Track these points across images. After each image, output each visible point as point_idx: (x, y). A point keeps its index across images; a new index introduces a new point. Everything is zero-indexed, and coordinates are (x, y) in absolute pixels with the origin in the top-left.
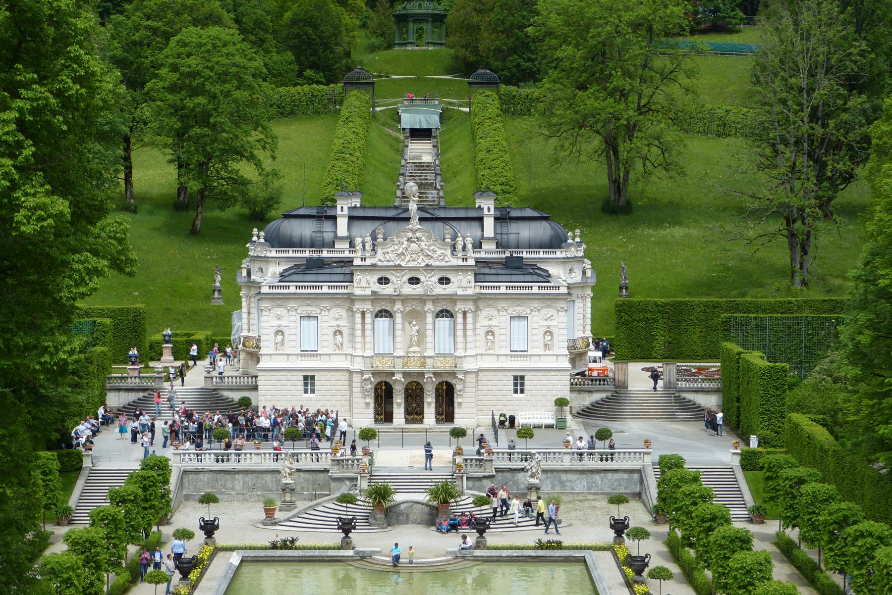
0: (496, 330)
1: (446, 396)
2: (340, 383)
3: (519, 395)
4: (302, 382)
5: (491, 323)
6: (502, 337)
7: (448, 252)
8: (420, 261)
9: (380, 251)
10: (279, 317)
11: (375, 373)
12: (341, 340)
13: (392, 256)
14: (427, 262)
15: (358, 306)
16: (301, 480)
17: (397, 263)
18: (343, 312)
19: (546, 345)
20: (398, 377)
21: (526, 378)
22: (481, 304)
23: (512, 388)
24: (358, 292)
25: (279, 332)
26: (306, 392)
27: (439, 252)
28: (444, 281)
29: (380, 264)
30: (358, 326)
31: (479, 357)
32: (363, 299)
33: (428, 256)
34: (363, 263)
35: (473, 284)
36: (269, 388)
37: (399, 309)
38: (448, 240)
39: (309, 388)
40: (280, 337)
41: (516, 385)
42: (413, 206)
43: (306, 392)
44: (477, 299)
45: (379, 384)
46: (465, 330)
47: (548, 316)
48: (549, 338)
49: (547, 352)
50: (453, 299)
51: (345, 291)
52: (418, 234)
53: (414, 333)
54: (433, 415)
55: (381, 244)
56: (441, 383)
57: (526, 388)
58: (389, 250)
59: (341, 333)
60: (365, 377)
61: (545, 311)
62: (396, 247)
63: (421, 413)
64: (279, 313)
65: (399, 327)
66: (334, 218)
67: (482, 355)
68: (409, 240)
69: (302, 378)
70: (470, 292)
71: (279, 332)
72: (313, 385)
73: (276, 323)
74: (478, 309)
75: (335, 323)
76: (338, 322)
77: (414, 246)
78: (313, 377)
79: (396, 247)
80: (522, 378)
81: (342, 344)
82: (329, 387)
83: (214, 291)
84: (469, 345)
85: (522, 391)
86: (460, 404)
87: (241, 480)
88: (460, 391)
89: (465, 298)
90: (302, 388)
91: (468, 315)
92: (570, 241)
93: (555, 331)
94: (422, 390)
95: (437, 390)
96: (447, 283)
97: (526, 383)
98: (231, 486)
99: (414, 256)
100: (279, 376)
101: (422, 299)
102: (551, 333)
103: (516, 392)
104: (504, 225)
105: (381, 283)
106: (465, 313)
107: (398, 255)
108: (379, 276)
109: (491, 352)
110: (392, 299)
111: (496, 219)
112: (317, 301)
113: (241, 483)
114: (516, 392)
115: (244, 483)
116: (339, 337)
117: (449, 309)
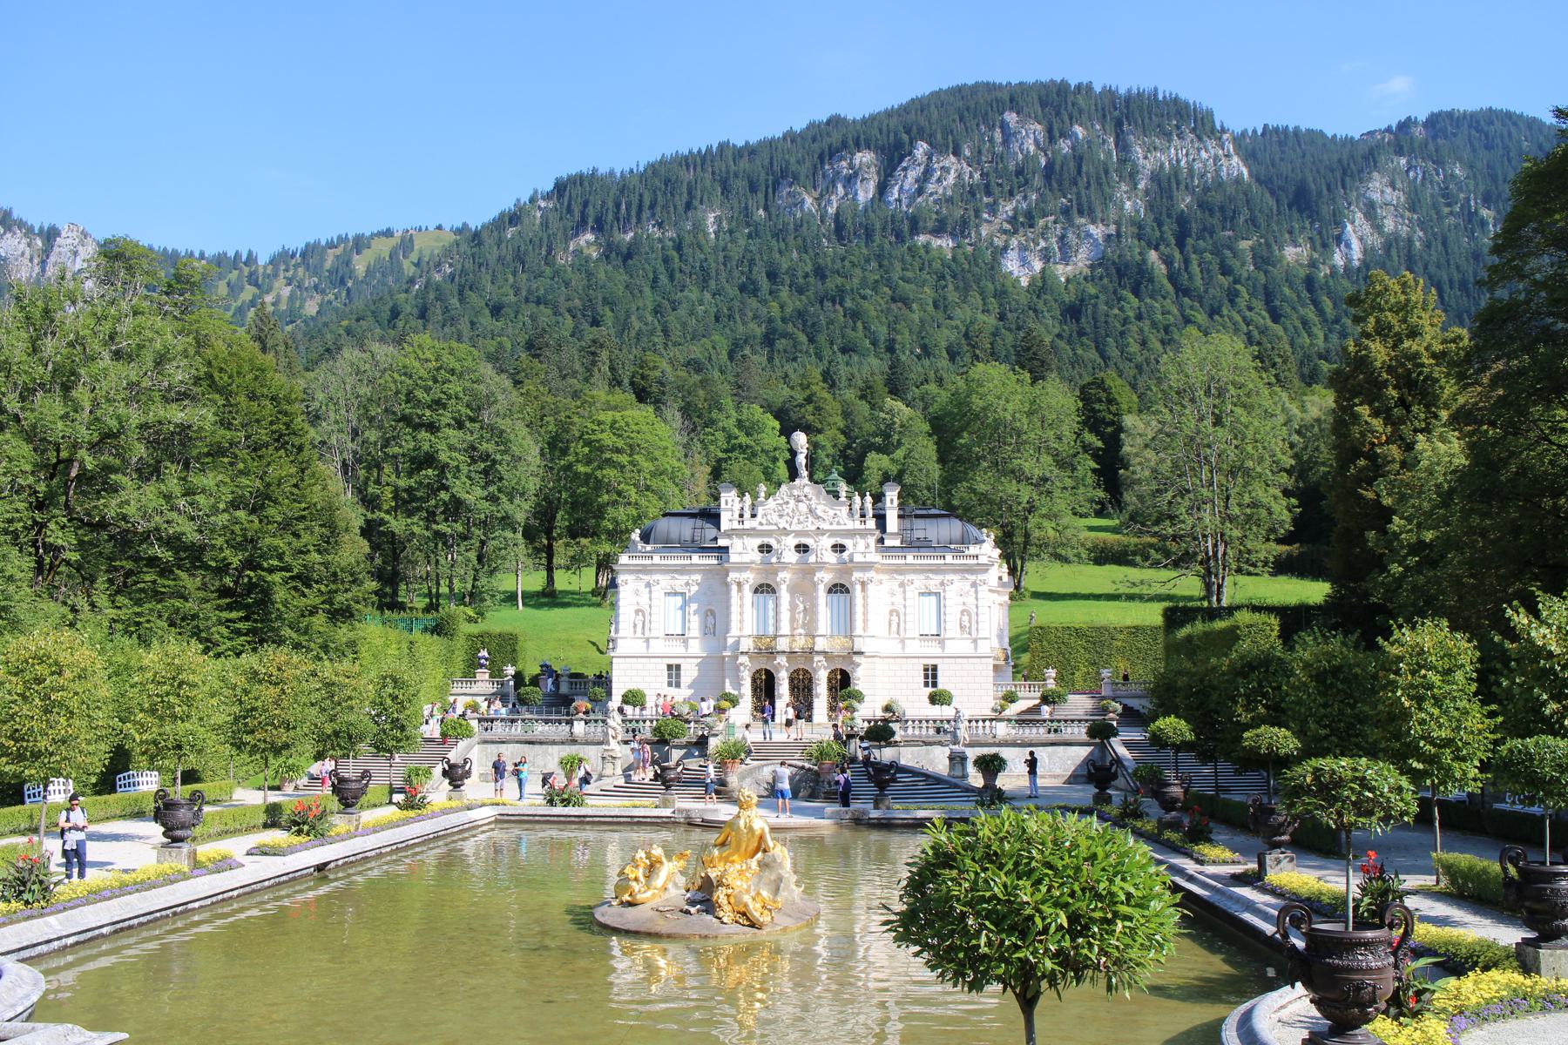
1: (842, 683)
5: (894, 599)
7: (845, 509)
10: (637, 592)
13: (775, 518)
20: (782, 660)
26: (670, 684)
27: (831, 513)
33: (818, 518)
41: (926, 676)
43: (670, 684)
63: (810, 707)
72: (678, 676)
77: (803, 507)
78: (678, 667)
80: (935, 668)
90: (666, 679)
91: (870, 587)
94: (810, 680)
97: (940, 673)
102: (969, 615)
104: (907, 522)
106: (863, 584)
108: (759, 541)
111: (900, 517)
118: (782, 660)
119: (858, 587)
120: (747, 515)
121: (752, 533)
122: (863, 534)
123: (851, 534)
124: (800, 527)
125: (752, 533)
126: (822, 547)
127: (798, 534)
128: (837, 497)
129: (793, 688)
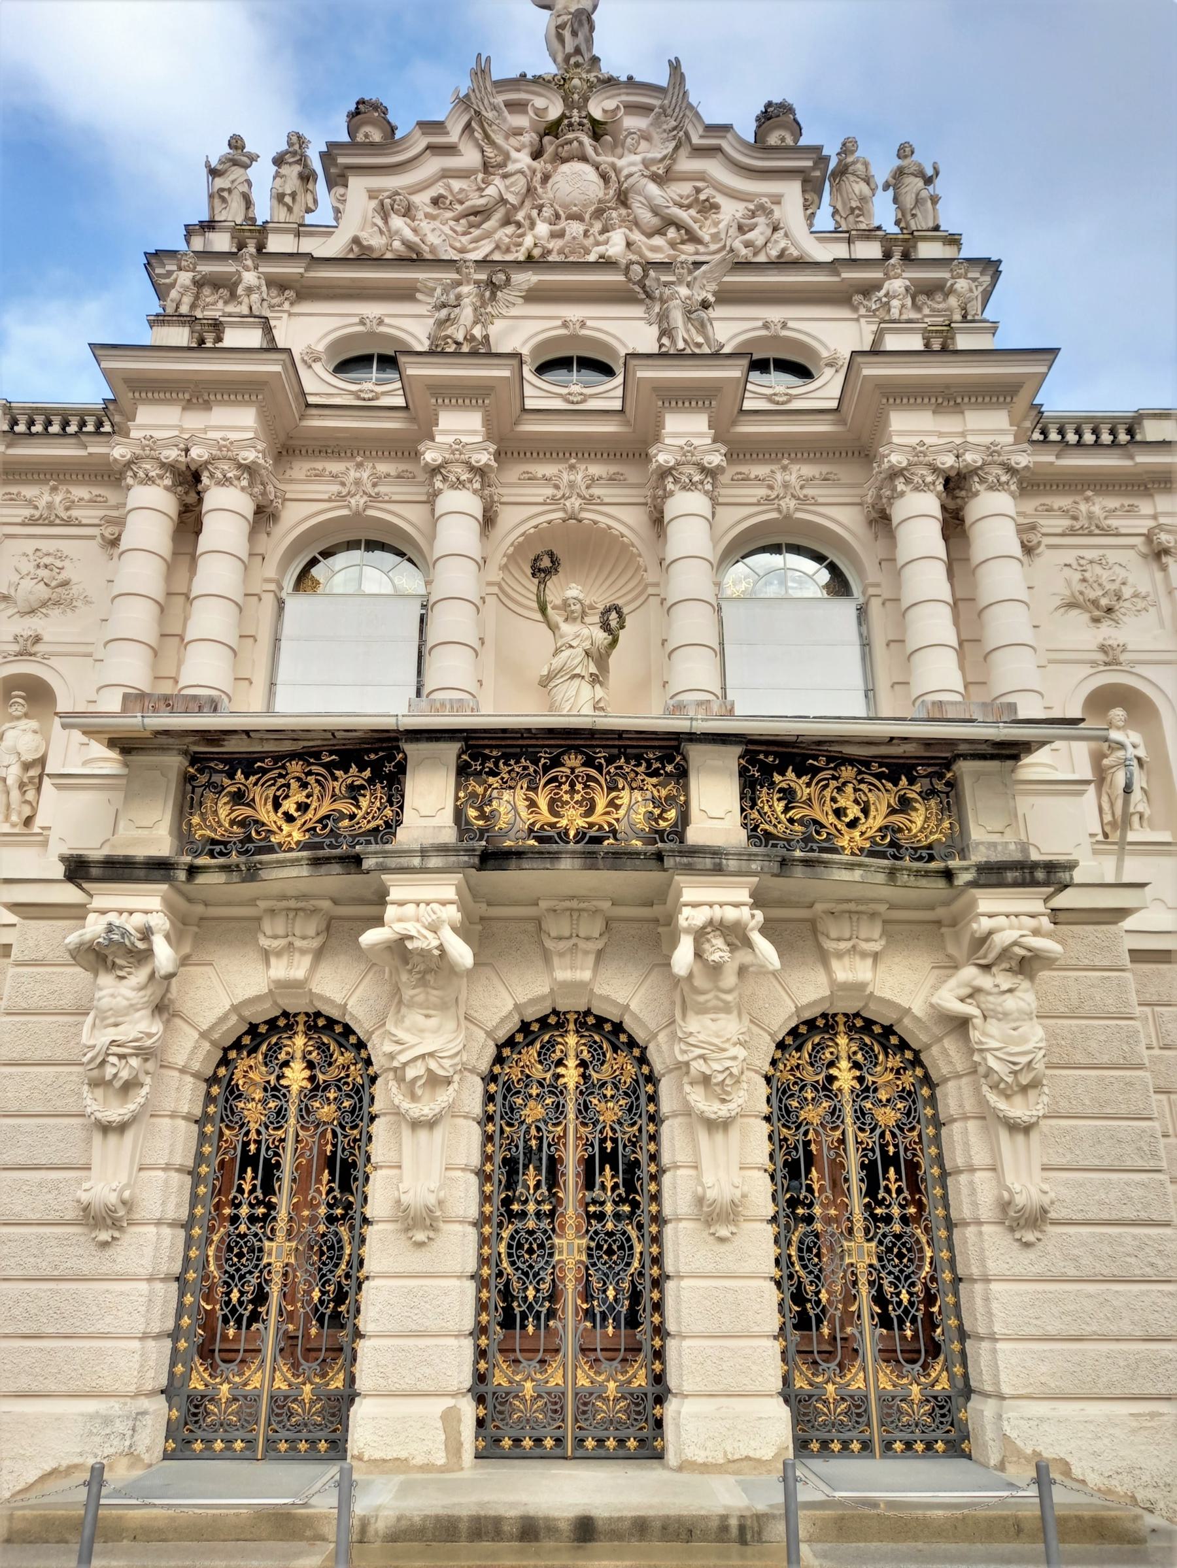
54: (765, 1360)
58: (422, 200)
65: (457, 579)
77: (576, 181)
86: (1024, 1221)
119: (919, 511)
129: (514, 1168)
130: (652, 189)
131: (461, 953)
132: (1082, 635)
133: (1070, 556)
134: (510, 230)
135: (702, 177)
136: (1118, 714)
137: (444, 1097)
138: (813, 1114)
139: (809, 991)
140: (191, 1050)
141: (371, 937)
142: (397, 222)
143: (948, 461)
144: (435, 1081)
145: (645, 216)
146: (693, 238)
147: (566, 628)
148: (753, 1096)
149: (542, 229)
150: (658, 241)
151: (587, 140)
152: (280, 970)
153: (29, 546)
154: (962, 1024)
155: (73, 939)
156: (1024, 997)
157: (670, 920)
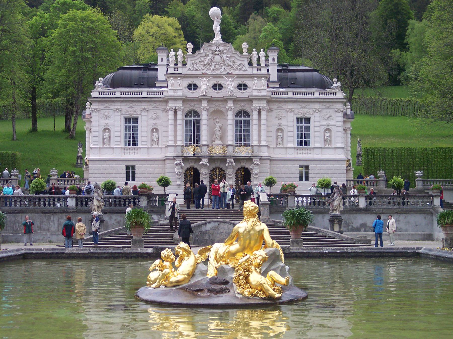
0: (285, 128)
2: (156, 171)
3: (304, 182)
4: (125, 171)
5: (280, 122)
6: (290, 134)
8: (222, 70)
9: (189, 62)
10: (107, 118)
11: (185, 159)
12: (157, 136)
13: (200, 66)
14: (228, 71)
15: (171, 104)
16: (113, 222)
17: (204, 72)
18: (160, 113)
19: (325, 140)
20: (204, 161)
21: (310, 167)
22: (272, 106)
23: (298, 175)
24: (171, 93)
25: (106, 129)
27: (238, 63)
28: (242, 87)
29: (190, 72)
30: (171, 122)
31: (271, 150)
32: (175, 99)
33: (229, 66)
34: (176, 72)
35: (265, 87)
36: (97, 175)
37: (205, 107)
38: (245, 53)
39: (131, 176)
40: (107, 134)
42: (217, 27)
44: (269, 101)
45: (188, 170)
46: (259, 126)
47: (328, 116)
48: (328, 134)
49: (327, 146)
50: (250, 100)
51: (161, 96)
52: (221, 48)
53: (217, 128)
55: (190, 56)
56: (239, 170)
57: (310, 176)
58: (197, 61)
59: (157, 130)
60: (177, 162)
61: (325, 112)
62: (203, 59)
64: (106, 114)
66: (157, 69)
67: (274, 148)
68: (214, 53)
69: (124, 167)
70: (264, 93)
71: (106, 129)
72: (134, 173)
73: (104, 122)
74: (269, 110)
75: (152, 122)
76: (154, 122)
77: (217, 58)
78: (133, 167)
79: (203, 59)
80: (307, 167)
81: (158, 139)
82: (146, 175)
83: (77, 159)
84: (263, 138)
85: (307, 179)
87: (56, 222)
88: (256, 174)
89: (259, 99)
90: (125, 175)
91: (263, 113)
92: (335, 85)
93: (333, 128)
95: (237, 176)
96: (245, 89)
97: (310, 171)
98: (46, 227)
99: (217, 66)
100: (106, 165)
101: (225, 100)
103: (301, 179)
105: (190, 89)
106: (259, 111)
107: (205, 65)
109: (281, 146)
110: (199, 100)
111: (279, 71)
112: (139, 104)
113: (56, 225)
114: (301, 179)
115: (59, 225)
116: (155, 134)
117: (247, 109)
118: (204, 161)
120: (180, 65)
121: (183, 76)
122: (259, 77)
123: (252, 76)
124: (217, 72)
125: (183, 76)
126: (230, 86)
127: (215, 77)
128: (241, 52)
130: (227, 61)
131: (208, 164)
132: (277, 122)
133: (277, 111)
134: (209, 66)
135: (234, 57)
136: (280, 131)
137: (207, 176)
138: (240, 177)
139: (239, 166)
140: (184, 172)
141: (200, 163)
142: (195, 66)
143: (258, 108)
144: (206, 175)
145: (227, 64)
146: (233, 67)
147: (217, 124)
148: (234, 175)
149: (213, 66)
150: (228, 68)
151: (219, 53)
152: (191, 165)
153: (153, 111)
154: (252, 169)
155: (175, 163)
156: (257, 167)
157: (226, 160)
